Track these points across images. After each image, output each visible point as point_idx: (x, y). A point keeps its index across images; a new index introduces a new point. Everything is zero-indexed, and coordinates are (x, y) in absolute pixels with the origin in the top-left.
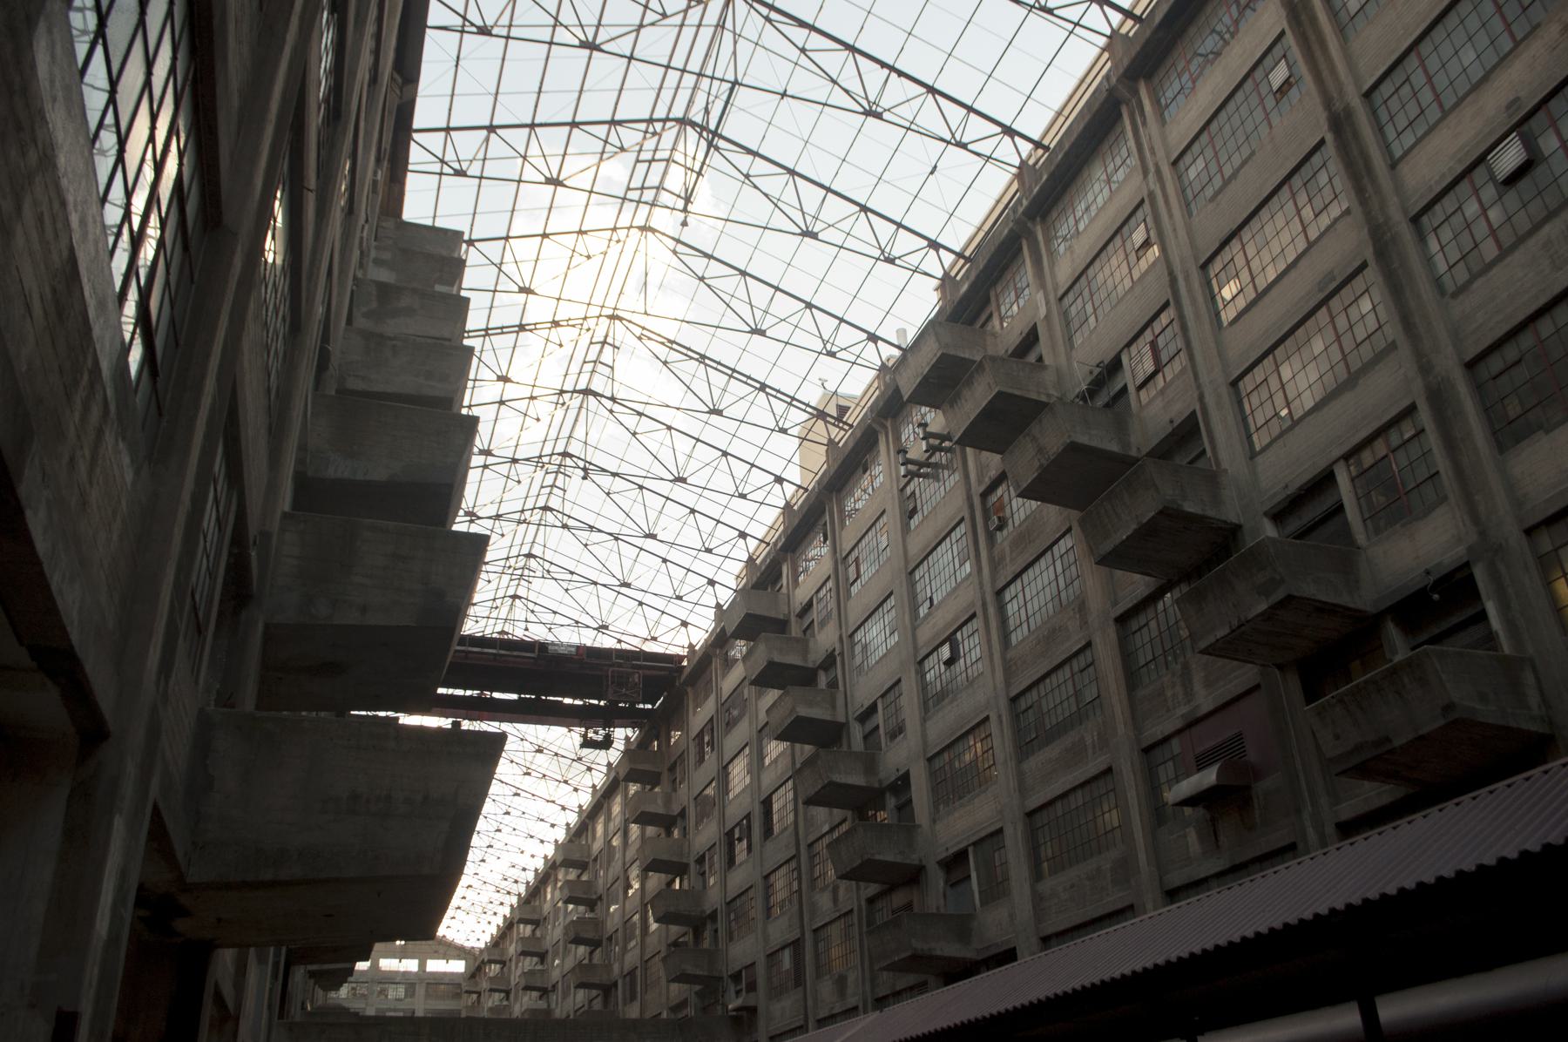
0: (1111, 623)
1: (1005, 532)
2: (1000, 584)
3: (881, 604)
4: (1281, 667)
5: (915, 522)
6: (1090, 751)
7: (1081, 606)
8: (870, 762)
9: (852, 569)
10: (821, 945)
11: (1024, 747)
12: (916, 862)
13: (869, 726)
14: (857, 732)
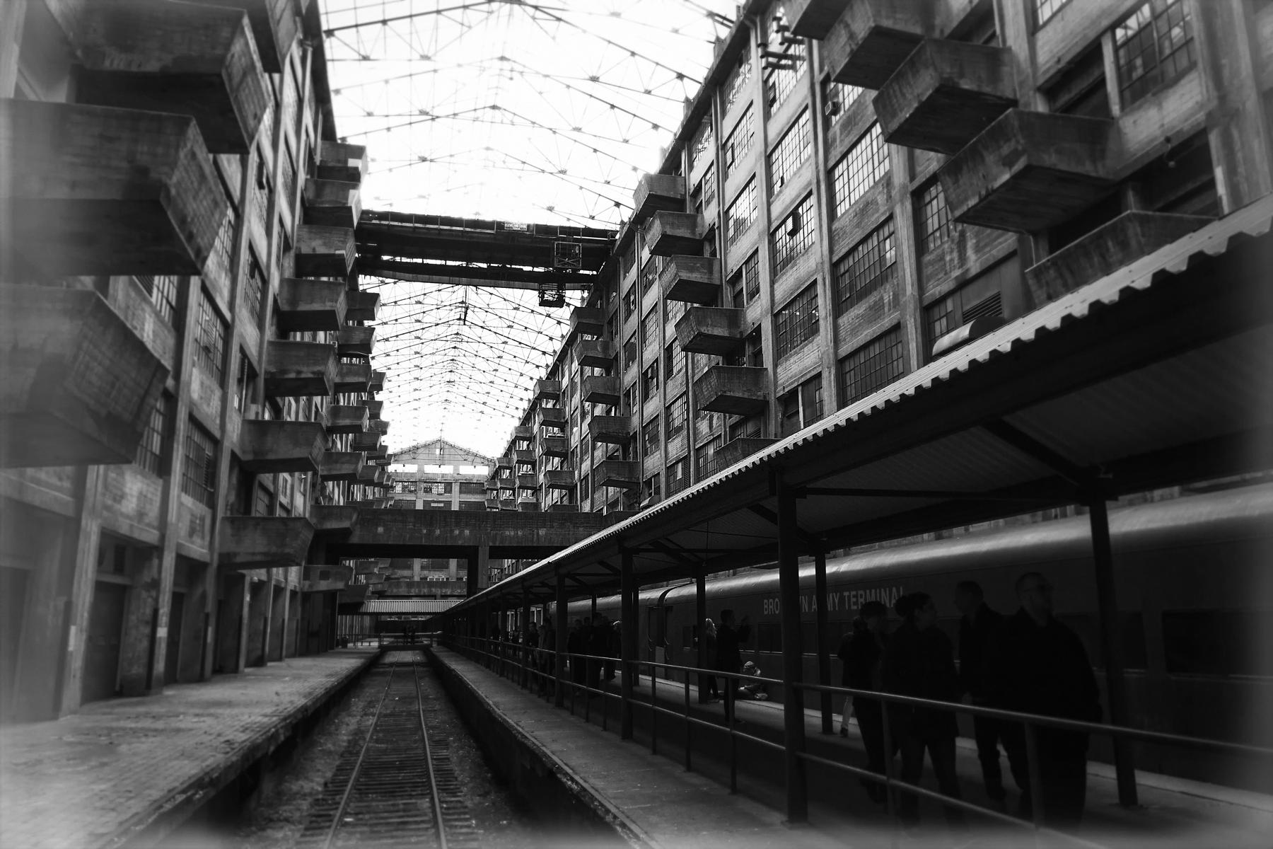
0: (908, 196)
1: (838, 117)
2: (831, 163)
3: (747, 185)
4: (1035, 235)
5: (774, 109)
6: (886, 309)
7: (887, 180)
8: (735, 317)
9: (729, 153)
10: (701, 460)
11: (838, 309)
12: (761, 398)
13: (738, 288)
14: (728, 294)
